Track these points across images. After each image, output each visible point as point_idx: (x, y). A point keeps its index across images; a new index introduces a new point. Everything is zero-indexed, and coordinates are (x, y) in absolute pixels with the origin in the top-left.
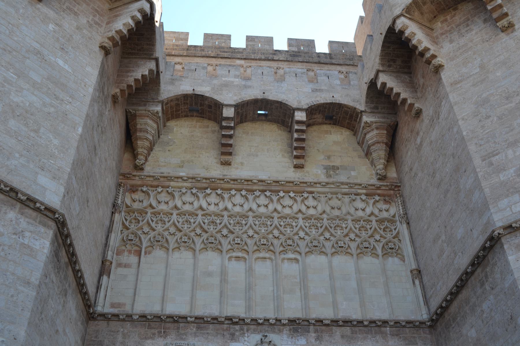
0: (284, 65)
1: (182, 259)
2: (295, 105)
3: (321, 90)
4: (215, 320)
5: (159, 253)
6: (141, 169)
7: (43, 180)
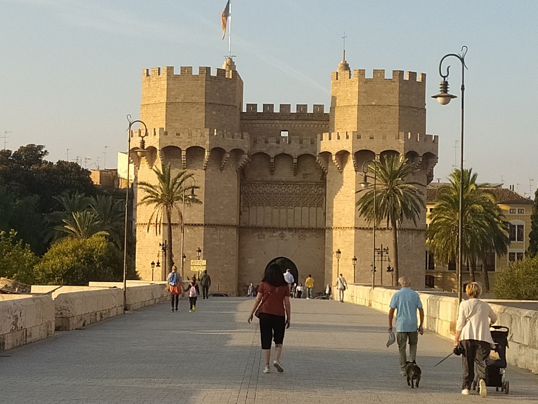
0: (294, 122)
1: (260, 208)
2: (293, 155)
3: (303, 148)
4: (270, 228)
5: (254, 207)
6: (246, 178)
7: (233, 219)
